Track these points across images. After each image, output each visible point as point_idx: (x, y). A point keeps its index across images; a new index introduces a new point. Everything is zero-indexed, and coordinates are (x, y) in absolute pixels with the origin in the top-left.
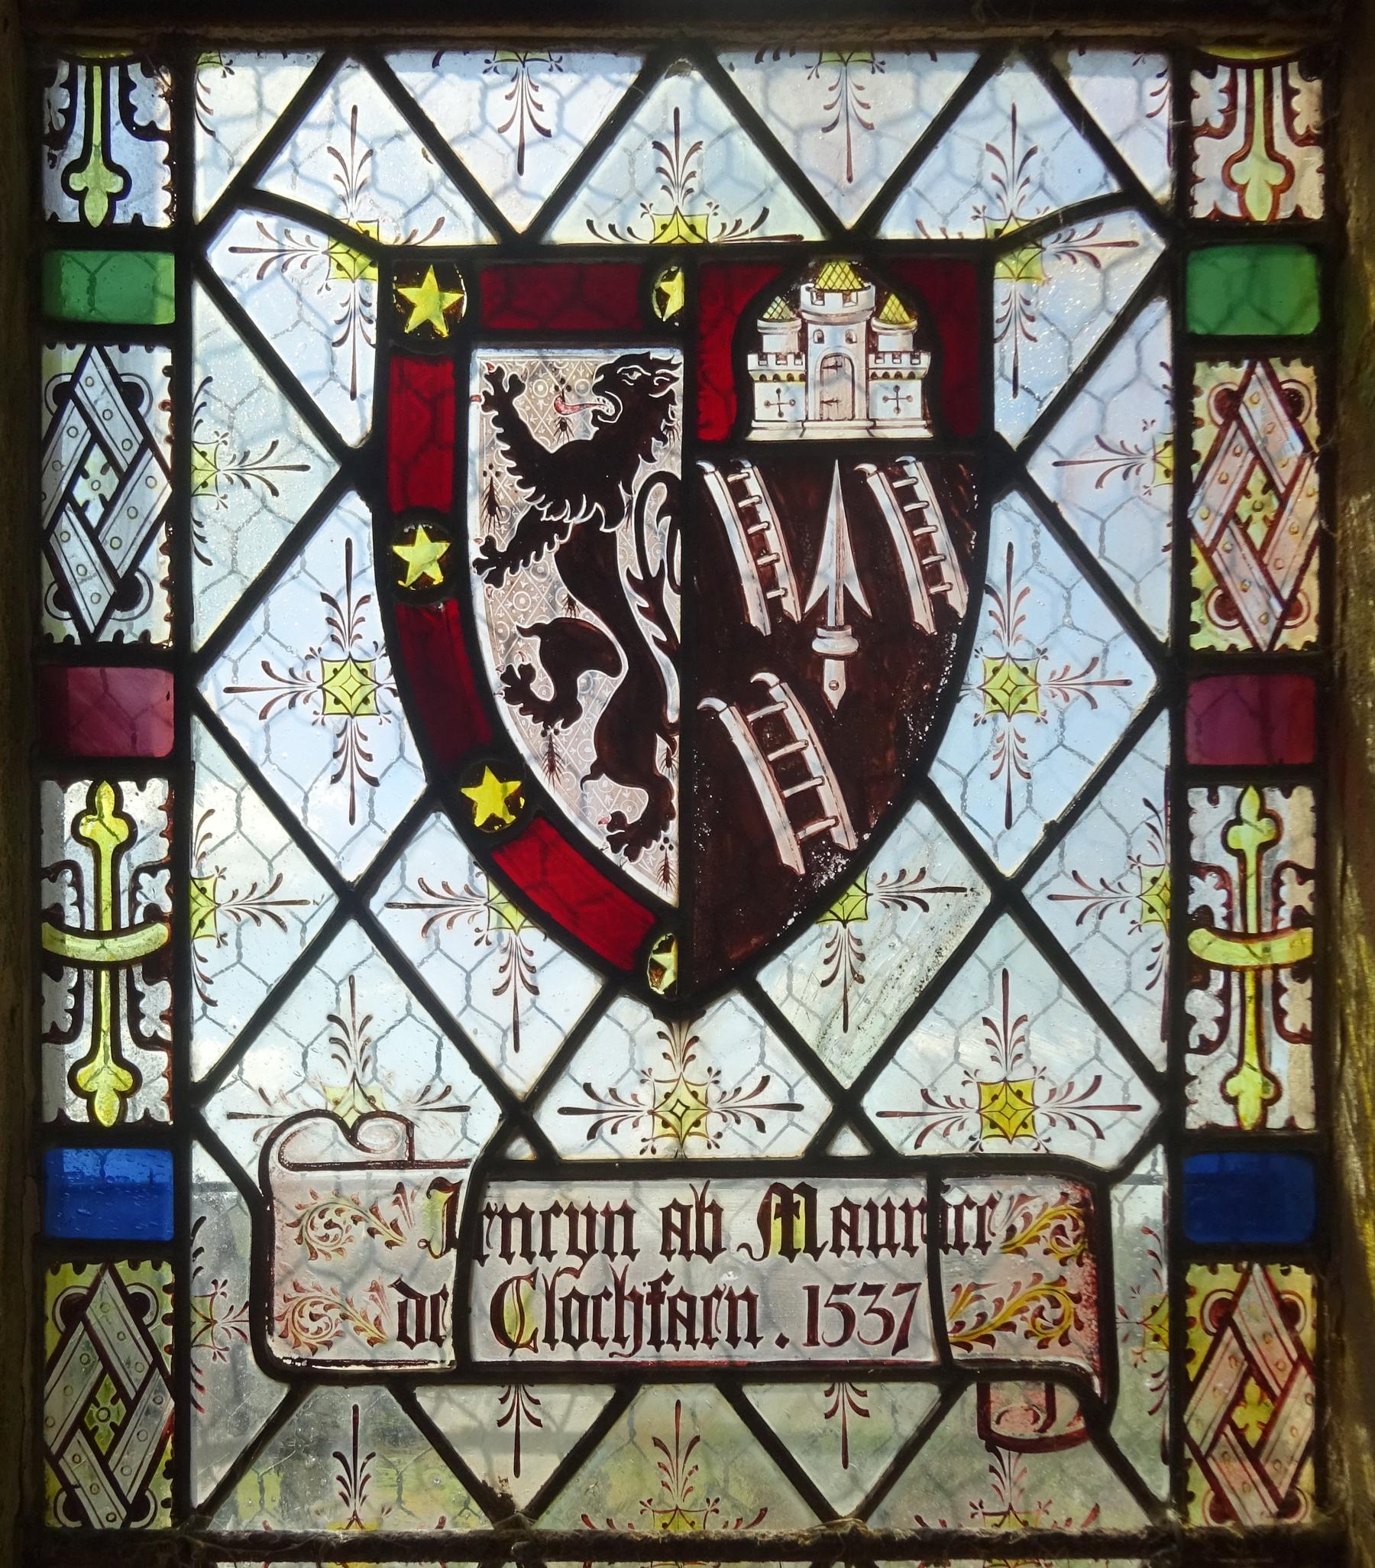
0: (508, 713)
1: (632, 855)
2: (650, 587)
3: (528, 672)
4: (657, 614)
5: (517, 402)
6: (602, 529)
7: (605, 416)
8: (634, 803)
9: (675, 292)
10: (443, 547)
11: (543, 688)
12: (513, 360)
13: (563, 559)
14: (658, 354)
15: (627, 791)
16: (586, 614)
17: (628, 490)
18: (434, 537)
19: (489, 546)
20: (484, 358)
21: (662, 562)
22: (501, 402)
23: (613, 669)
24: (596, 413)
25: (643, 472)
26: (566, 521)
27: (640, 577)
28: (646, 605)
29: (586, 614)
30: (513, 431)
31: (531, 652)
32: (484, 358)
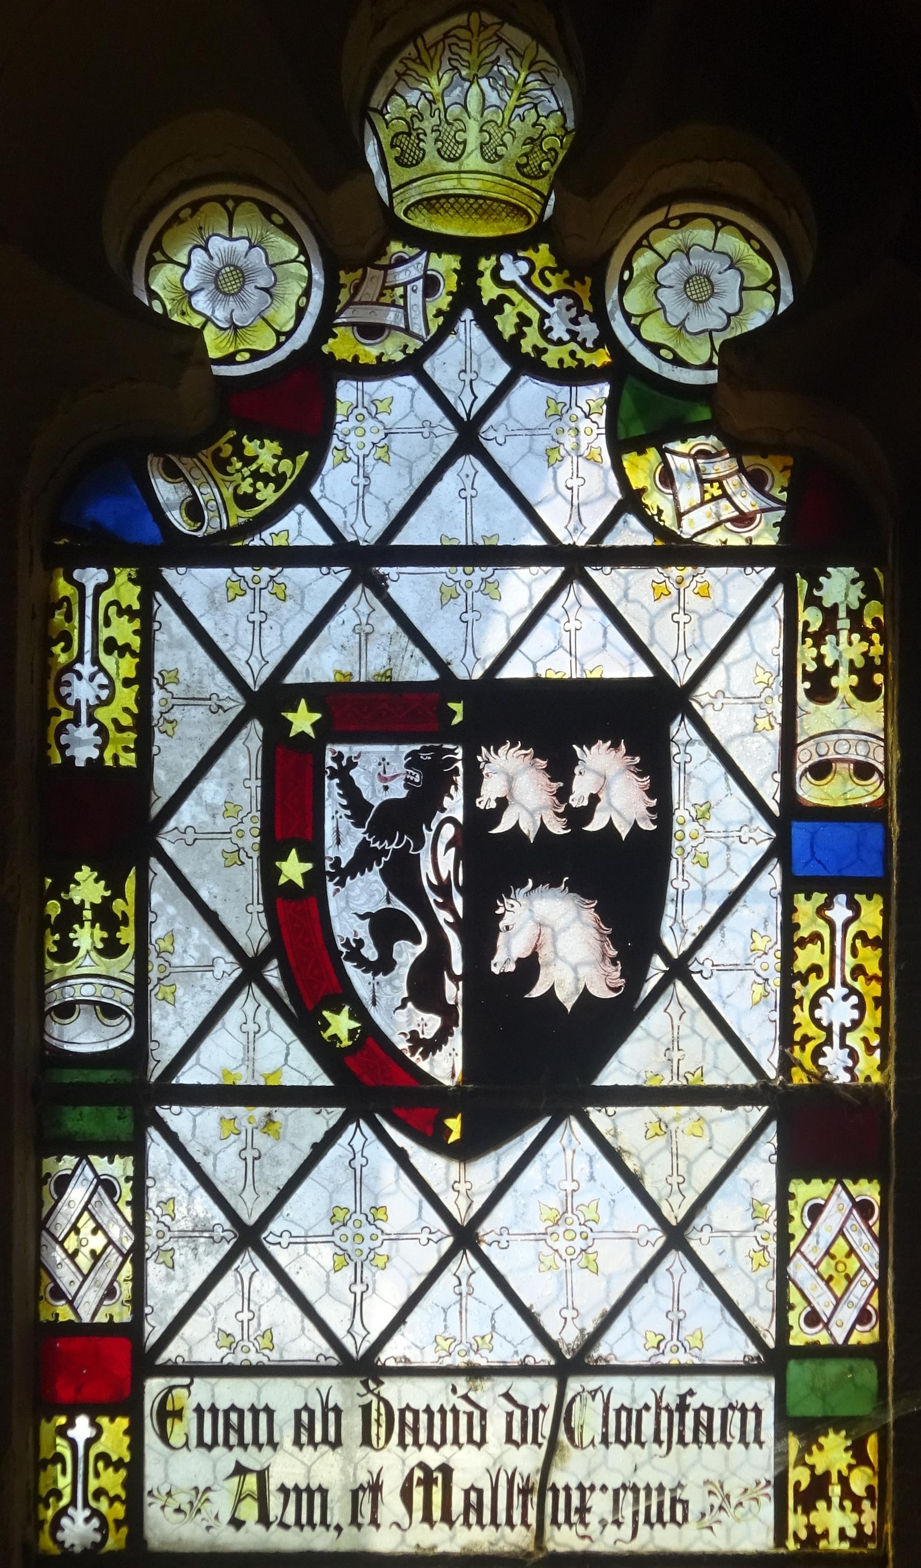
2: (443, 889)
3: (360, 943)
4: (448, 905)
5: (353, 773)
6: (411, 852)
7: (413, 781)
8: (431, 1024)
10: (308, 866)
11: (370, 952)
13: (385, 874)
16: (399, 905)
17: (430, 829)
18: (302, 859)
21: (449, 872)
22: (343, 774)
23: (417, 940)
24: (407, 780)
26: (387, 848)
27: (435, 882)
28: (440, 900)
29: (399, 905)
31: (363, 930)
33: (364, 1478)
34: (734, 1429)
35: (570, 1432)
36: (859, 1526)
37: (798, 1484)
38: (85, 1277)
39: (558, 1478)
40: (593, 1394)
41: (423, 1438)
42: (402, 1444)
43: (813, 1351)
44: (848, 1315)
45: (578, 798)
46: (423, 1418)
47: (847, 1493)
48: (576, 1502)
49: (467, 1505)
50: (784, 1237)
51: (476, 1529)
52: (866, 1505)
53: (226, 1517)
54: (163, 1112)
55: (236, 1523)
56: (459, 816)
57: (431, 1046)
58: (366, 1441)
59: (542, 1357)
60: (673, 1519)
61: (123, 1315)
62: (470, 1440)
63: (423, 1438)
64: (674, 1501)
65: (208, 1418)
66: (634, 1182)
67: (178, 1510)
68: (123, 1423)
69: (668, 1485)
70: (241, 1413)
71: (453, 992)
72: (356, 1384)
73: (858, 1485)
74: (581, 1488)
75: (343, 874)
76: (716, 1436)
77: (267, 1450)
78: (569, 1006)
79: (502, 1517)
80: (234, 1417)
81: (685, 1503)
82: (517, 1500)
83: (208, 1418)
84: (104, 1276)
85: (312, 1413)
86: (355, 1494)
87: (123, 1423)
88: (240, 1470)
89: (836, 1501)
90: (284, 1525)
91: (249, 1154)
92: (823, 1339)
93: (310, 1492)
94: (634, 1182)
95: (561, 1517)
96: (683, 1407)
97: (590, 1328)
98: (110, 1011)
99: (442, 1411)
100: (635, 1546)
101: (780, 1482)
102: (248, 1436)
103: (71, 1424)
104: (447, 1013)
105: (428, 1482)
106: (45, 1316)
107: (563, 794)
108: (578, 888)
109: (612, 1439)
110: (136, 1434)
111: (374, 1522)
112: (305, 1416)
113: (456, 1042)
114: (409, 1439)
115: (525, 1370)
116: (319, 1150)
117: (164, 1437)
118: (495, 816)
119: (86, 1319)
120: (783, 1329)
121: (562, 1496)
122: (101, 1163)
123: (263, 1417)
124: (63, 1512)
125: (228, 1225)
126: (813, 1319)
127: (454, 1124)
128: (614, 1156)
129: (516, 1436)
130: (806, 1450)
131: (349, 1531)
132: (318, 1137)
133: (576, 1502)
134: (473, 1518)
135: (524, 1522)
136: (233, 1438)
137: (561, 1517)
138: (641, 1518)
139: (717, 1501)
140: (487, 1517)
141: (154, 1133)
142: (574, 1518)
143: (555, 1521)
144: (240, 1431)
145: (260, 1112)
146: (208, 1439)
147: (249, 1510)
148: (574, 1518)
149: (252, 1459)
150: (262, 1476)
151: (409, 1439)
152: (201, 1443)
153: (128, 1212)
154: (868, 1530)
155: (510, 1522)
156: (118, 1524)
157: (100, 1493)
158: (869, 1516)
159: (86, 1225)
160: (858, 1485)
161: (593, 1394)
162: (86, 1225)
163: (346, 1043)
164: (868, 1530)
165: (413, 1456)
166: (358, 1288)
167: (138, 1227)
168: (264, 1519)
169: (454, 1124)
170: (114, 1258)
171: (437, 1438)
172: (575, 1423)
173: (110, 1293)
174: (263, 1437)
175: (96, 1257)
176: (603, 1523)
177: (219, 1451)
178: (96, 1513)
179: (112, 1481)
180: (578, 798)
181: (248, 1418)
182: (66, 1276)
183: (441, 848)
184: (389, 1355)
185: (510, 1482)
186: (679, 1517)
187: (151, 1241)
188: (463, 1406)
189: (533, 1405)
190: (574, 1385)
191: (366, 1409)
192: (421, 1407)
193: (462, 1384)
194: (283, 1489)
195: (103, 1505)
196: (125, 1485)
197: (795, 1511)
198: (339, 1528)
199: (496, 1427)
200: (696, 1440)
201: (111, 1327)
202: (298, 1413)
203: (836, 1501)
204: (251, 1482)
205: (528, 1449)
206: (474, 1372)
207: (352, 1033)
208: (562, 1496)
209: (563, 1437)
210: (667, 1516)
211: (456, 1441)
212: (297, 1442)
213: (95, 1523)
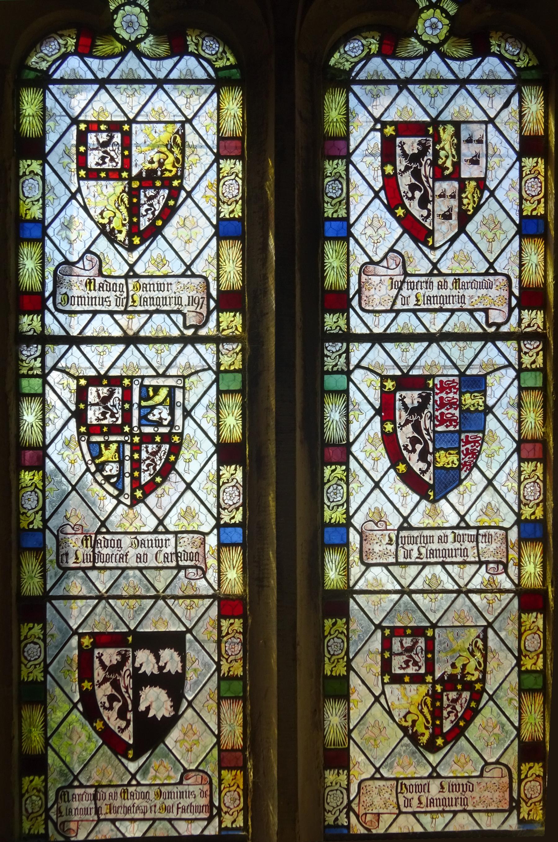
0: (101, 709)
1: (122, 733)
3: (105, 703)
8: (123, 724)
9: (130, 639)
11: (107, 705)
12: (101, 651)
13: (111, 684)
14: (128, 649)
15: (121, 722)
19: (98, 681)
20: (96, 652)
22: (100, 658)
23: (119, 701)
25: (125, 669)
30: (102, 663)
31: (105, 699)
32: (96, 652)
45: (161, 664)
56: (131, 669)
71: (130, 716)
75: (100, 684)
107: (158, 662)
108: (162, 687)
113: (131, 728)
118: (140, 668)
180: (161, 664)
183: (126, 676)
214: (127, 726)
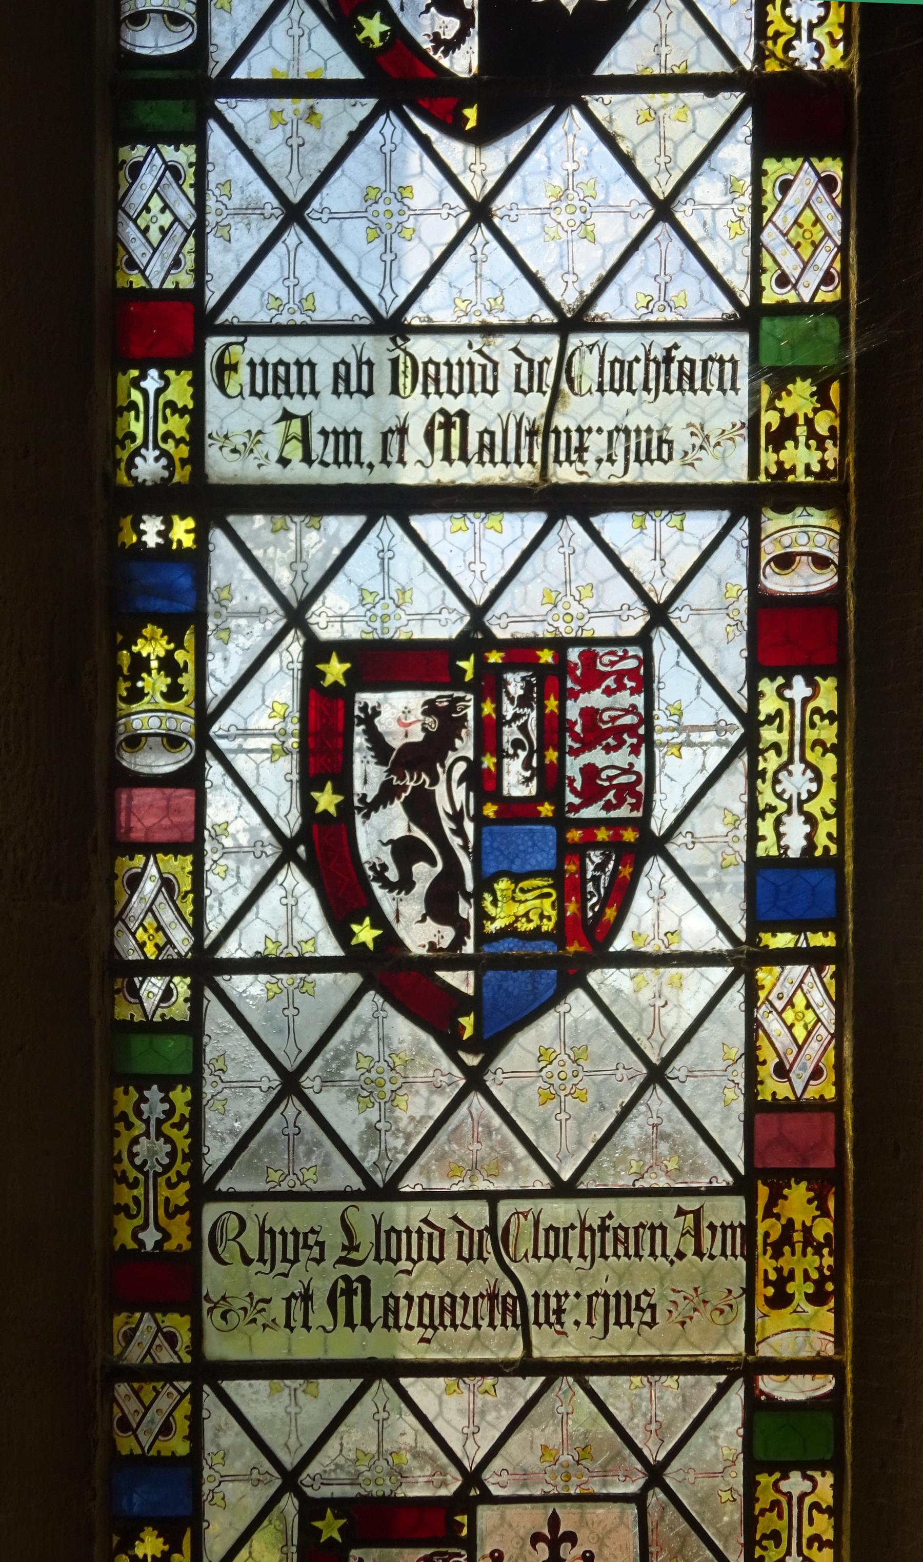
8: (450, 26)
33: (394, 423)
34: (714, 379)
35: (570, 381)
36: (823, 462)
37: (769, 425)
38: (155, 250)
39: (560, 421)
40: (591, 348)
41: (443, 387)
42: (426, 393)
43: (782, 310)
44: (813, 277)
46: (444, 370)
47: (812, 433)
48: (575, 442)
49: (482, 446)
50: (758, 209)
51: (489, 466)
52: (829, 444)
53: (274, 456)
54: (221, 104)
55: (284, 462)
57: (451, 46)
58: (395, 390)
59: (546, 316)
60: (660, 458)
61: (186, 281)
62: (484, 390)
63: (443, 387)
64: (661, 441)
65: (259, 370)
66: (627, 162)
67: (234, 451)
68: (187, 376)
69: (655, 427)
70: (287, 366)
72: (385, 342)
73: (822, 428)
74: (580, 430)
76: (698, 384)
77: (310, 398)
78: (570, 9)
79: (511, 456)
80: (281, 370)
81: (670, 443)
82: (525, 441)
83: (259, 370)
84: (169, 250)
85: (348, 366)
86: (385, 435)
87: (187, 376)
88: (287, 416)
89: (802, 440)
90: (325, 464)
91: (295, 142)
92: (792, 298)
93: (346, 434)
94: (627, 162)
95: (562, 456)
96: (668, 360)
97: (588, 290)
98: (175, 19)
99: (460, 364)
100: (628, 479)
101: (754, 423)
102: (294, 387)
103: (143, 376)
104: (466, 17)
105: (447, 426)
106: (121, 283)
109: (607, 387)
110: (198, 385)
111: (401, 461)
112: (342, 369)
113: (472, 44)
114: (431, 389)
115: (531, 328)
116: (355, 138)
117: (222, 388)
119: (156, 285)
120: (757, 290)
121: (563, 436)
122: (169, 152)
123: (306, 370)
124: (136, 453)
125: (276, 203)
126: (783, 280)
127: (471, 114)
128: (609, 139)
129: (524, 385)
130: (776, 395)
131: (380, 468)
132: (354, 126)
133: (575, 442)
134: (486, 457)
135: (531, 461)
136: (281, 388)
137: (562, 456)
138: (632, 456)
139: (698, 441)
140: (498, 457)
141: (213, 124)
142: (574, 457)
143: (557, 460)
144: (287, 382)
145: (302, 104)
146: (259, 389)
147: (294, 451)
148: (574, 457)
149: (298, 406)
150: (305, 421)
151: (431, 389)
152: (253, 393)
153: (191, 193)
154: (831, 466)
155: (518, 461)
156: (183, 462)
157: (168, 436)
158: (832, 453)
159: (156, 204)
160: (822, 428)
161: (591, 348)
162: (156, 204)
163: (377, 43)
164: (831, 466)
165: (435, 403)
166: (388, 257)
167: (200, 206)
168: (307, 459)
169: (471, 114)
170: (178, 230)
171: (455, 387)
172: (575, 373)
173: (177, 263)
174: (306, 388)
175: (164, 232)
176: (599, 461)
177: (270, 400)
178: (164, 453)
179: (178, 425)
181: (294, 370)
182: (139, 250)
184: (413, 317)
185: (519, 425)
186: (665, 456)
187: (211, 218)
188: (478, 360)
189: (538, 358)
190: (574, 340)
191: (395, 362)
192: (442, 360)
193: (477, 341)
194: (324, 432)
195: (170, 446)
196: (189, 429)
197: (767, 450)
198: (371, 466)
199: (506, 379)
200: (680, 387)
201: (177, 292)
202: (336, 366)
203: (802, 440)
204: (296, 427)
205: (534, 395)
206: (488, 330)
207: (383, 35)
208: (563, 436)
209: (564, 386)
210: (654, 455)
211: (472, 390)
212: (336, 392)
213: (164, 461)
214: (461, 37)
